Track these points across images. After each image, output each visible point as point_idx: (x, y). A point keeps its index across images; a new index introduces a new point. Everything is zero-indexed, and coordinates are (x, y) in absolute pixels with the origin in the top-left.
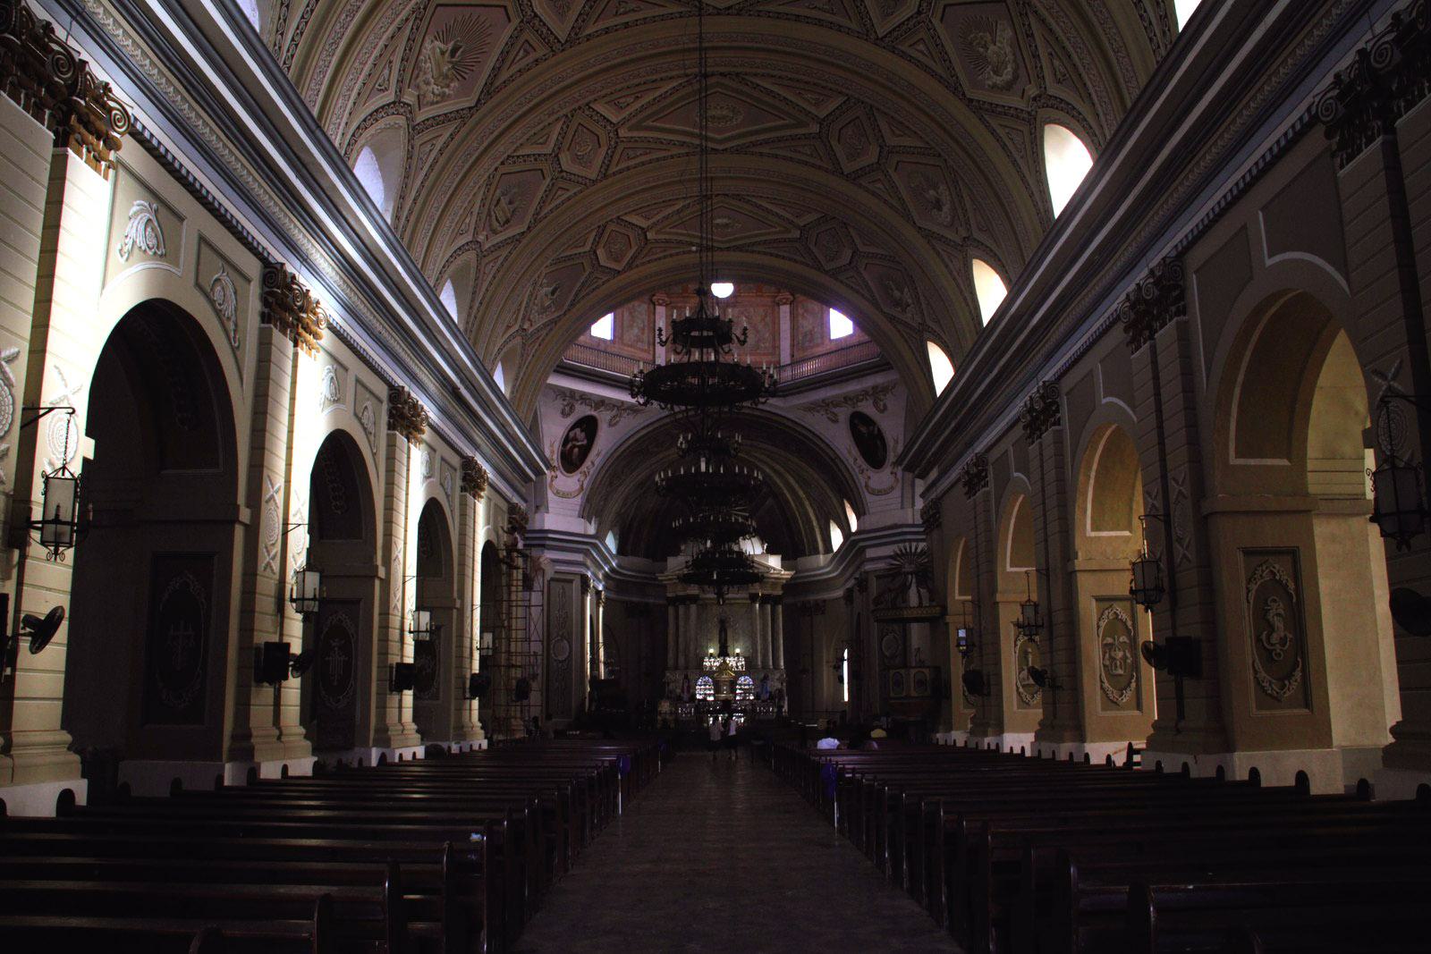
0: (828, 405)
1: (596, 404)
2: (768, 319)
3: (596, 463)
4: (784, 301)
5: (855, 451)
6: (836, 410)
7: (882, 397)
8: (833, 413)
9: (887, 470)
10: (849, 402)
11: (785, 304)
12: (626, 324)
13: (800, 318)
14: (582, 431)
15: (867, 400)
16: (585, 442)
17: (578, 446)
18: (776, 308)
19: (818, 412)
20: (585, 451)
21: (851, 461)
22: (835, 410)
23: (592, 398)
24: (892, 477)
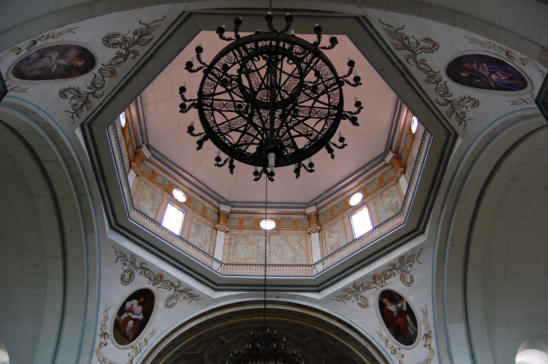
0: (358, 289)
1: (155, 278)
2: (302, 243)
3: (149, 342)
4: (314, 230)
5: (386, 333)
6: (365, 294)
7: (409, 269)
8: (363, 297)
9: (420, 342)
10: (379, 282)
11: (315, 232)
12: (191, 232)
13: (327, 238)
14: (139, 304)
15: (394, 275)
16: (141, 317)
17: (134, 320)
18: (308, 236)
19: (349, 299)
20: (140, 326)
21: (383, 343)
22: (364, 294)
23: (153, 269)
24: (426, 350)
